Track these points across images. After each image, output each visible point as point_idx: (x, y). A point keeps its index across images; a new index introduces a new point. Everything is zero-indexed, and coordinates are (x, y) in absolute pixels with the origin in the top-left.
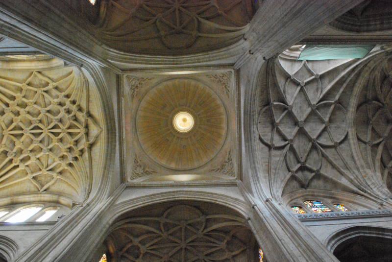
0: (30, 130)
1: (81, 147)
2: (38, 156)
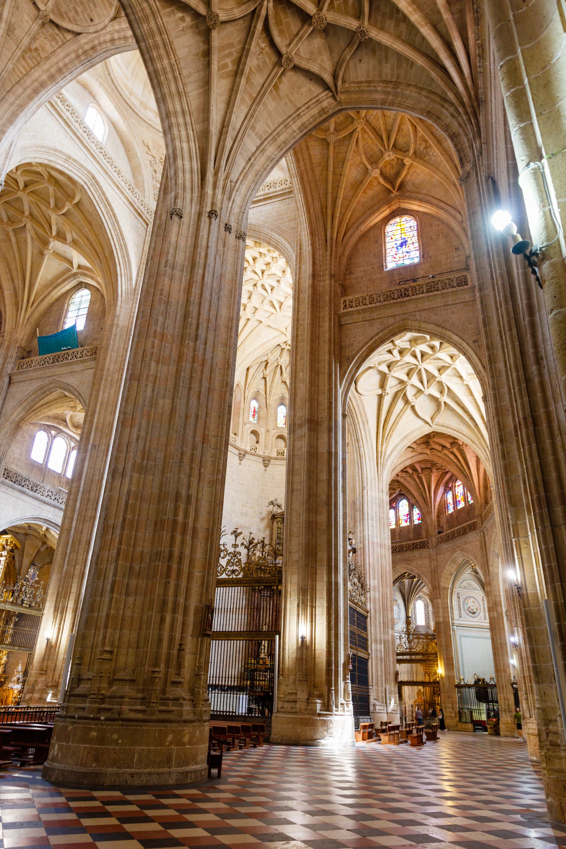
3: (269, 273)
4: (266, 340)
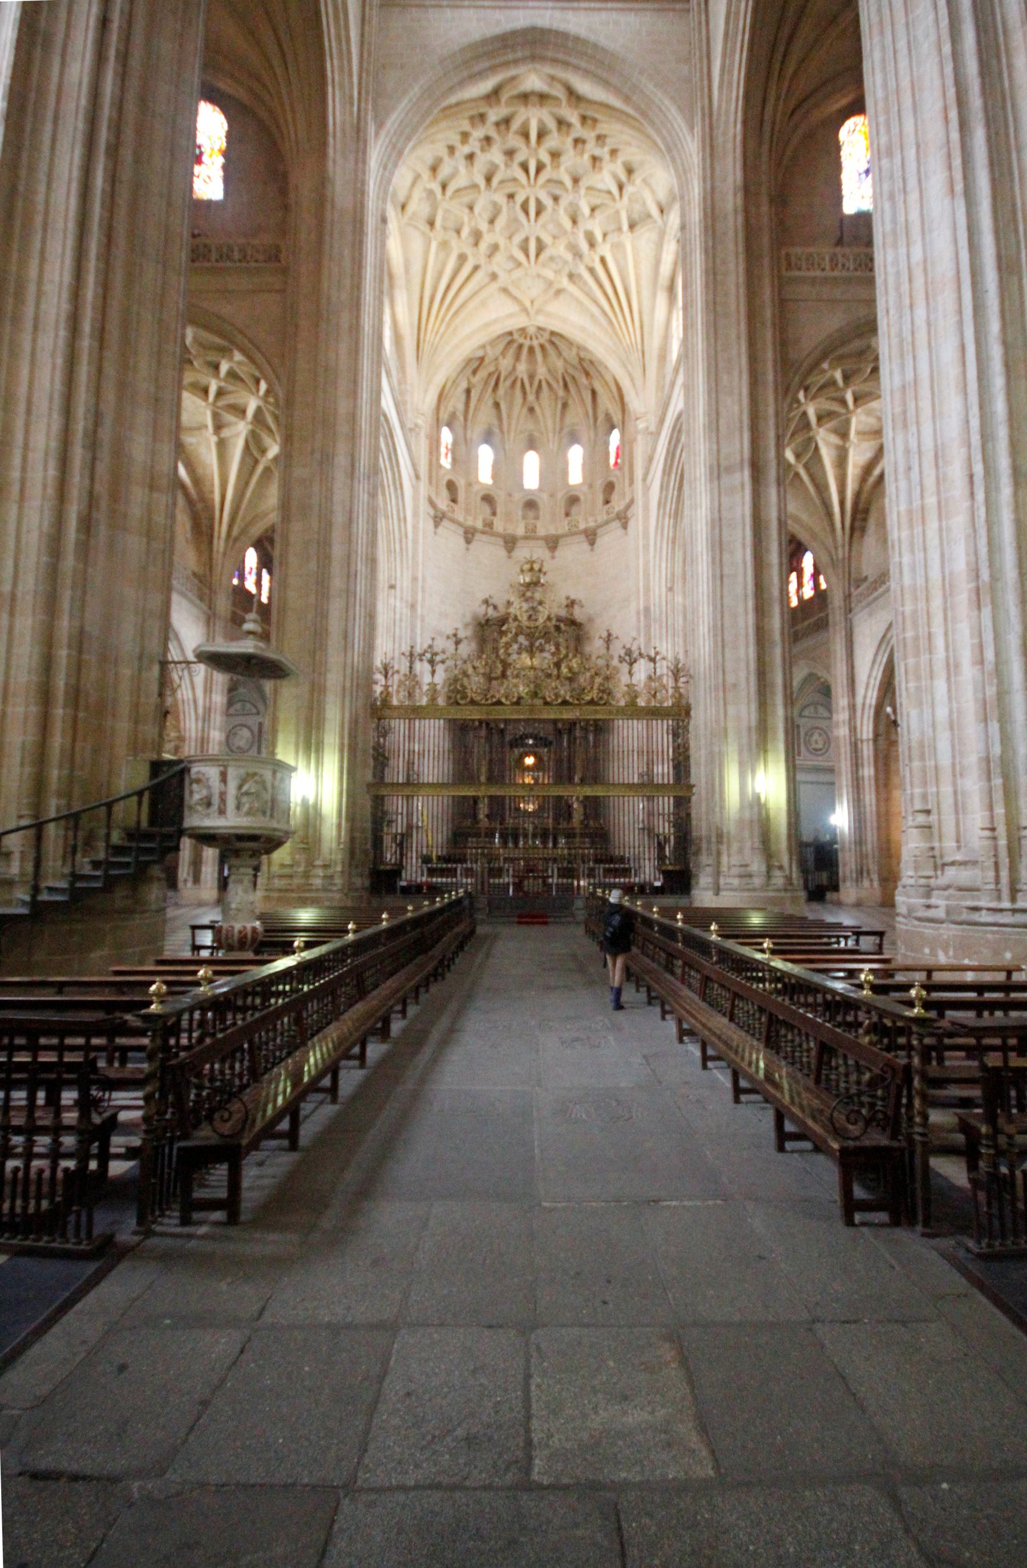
0: (529, 220)
1: (574, 119)
2: (586, 210)
3: (554, 176)
4: (493, 316)
